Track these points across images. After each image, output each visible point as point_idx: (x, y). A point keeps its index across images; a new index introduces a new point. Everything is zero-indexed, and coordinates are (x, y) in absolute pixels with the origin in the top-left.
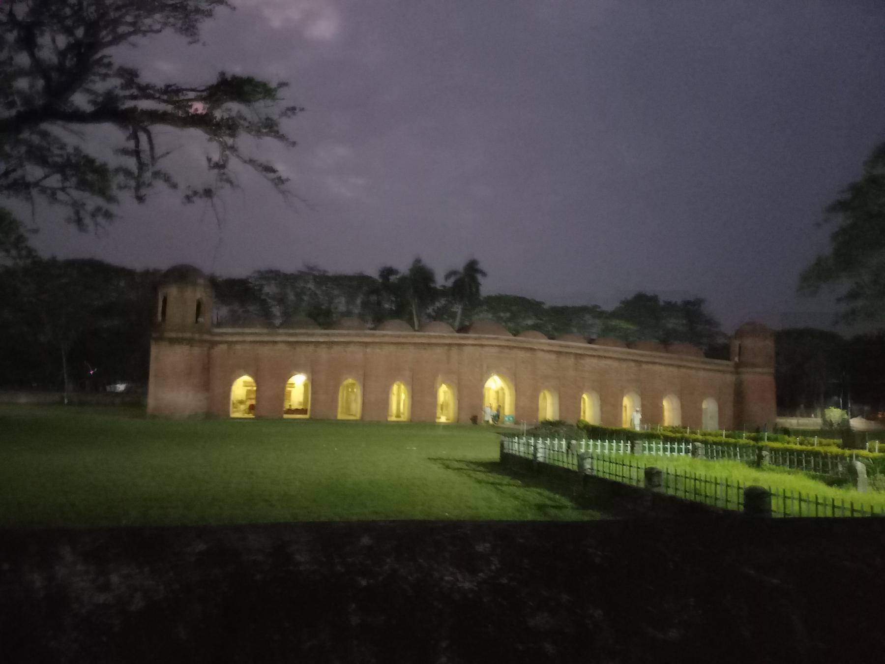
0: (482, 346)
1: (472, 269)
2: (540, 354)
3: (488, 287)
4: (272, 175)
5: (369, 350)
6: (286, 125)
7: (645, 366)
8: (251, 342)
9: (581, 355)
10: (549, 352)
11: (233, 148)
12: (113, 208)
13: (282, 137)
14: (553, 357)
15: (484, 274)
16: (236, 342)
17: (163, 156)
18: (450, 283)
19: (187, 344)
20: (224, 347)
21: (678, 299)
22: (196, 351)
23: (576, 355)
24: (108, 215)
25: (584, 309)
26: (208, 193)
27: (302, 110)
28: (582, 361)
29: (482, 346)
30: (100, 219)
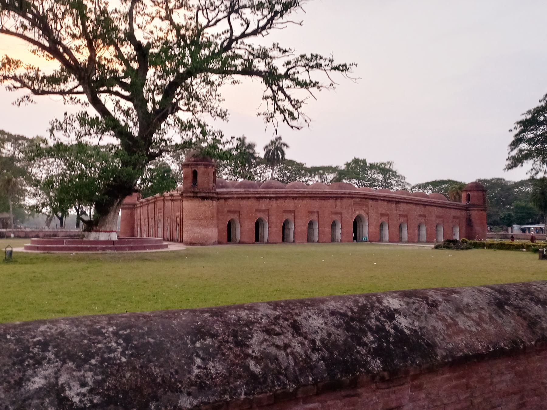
2: (379, 202)
10: (384, 200)
14: (386, 203)
23: (396, 202)
28: (399, 205)
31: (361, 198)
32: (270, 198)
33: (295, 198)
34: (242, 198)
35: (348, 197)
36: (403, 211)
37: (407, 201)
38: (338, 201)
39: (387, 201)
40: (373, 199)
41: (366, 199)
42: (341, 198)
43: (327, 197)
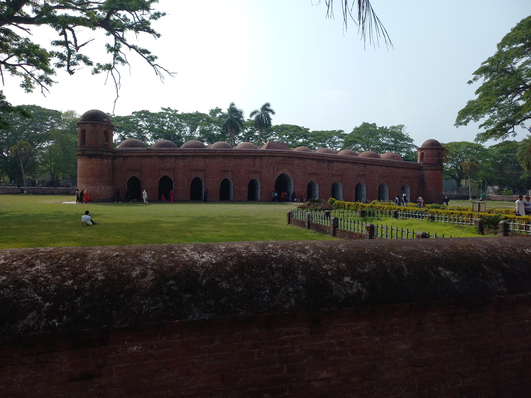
0: (274, 156)
1: (266, 108)
2: (308, 161)
3: (276, 121)
4: (146, 55)
5: (207, 160)
6: (154, 25)
7: (368, 167)
8: (137, 156)
9: (331, 161)
10: (313, 159)
11: (123, 40)
12: (51, 77)
13: (152, 32)
14: (315, 162)
15: (273, 113)
16: (128, 157)
17: (83, 45)
18: (253, 118)
19: (99, 158)
20: (121, 159)
21: (388, 125)
22: (105, 161)
23: (328, 161)
24: (49, 81)
25: (333, 133)
26: (109, 67)
27: (164, 14)
29: (274, 156)
30: (43, 83)
31: (284, 157)
32: (176, 157)
33: (205, 157)
34: (144, 157)
35: (268, 156)
36: (337, 171)
37: (343, 160)
38: (257, 161)
39: (317, 160)
40: (300, 158)
41: (291, 157)
42: (261, 156)
43: (242, 156)
